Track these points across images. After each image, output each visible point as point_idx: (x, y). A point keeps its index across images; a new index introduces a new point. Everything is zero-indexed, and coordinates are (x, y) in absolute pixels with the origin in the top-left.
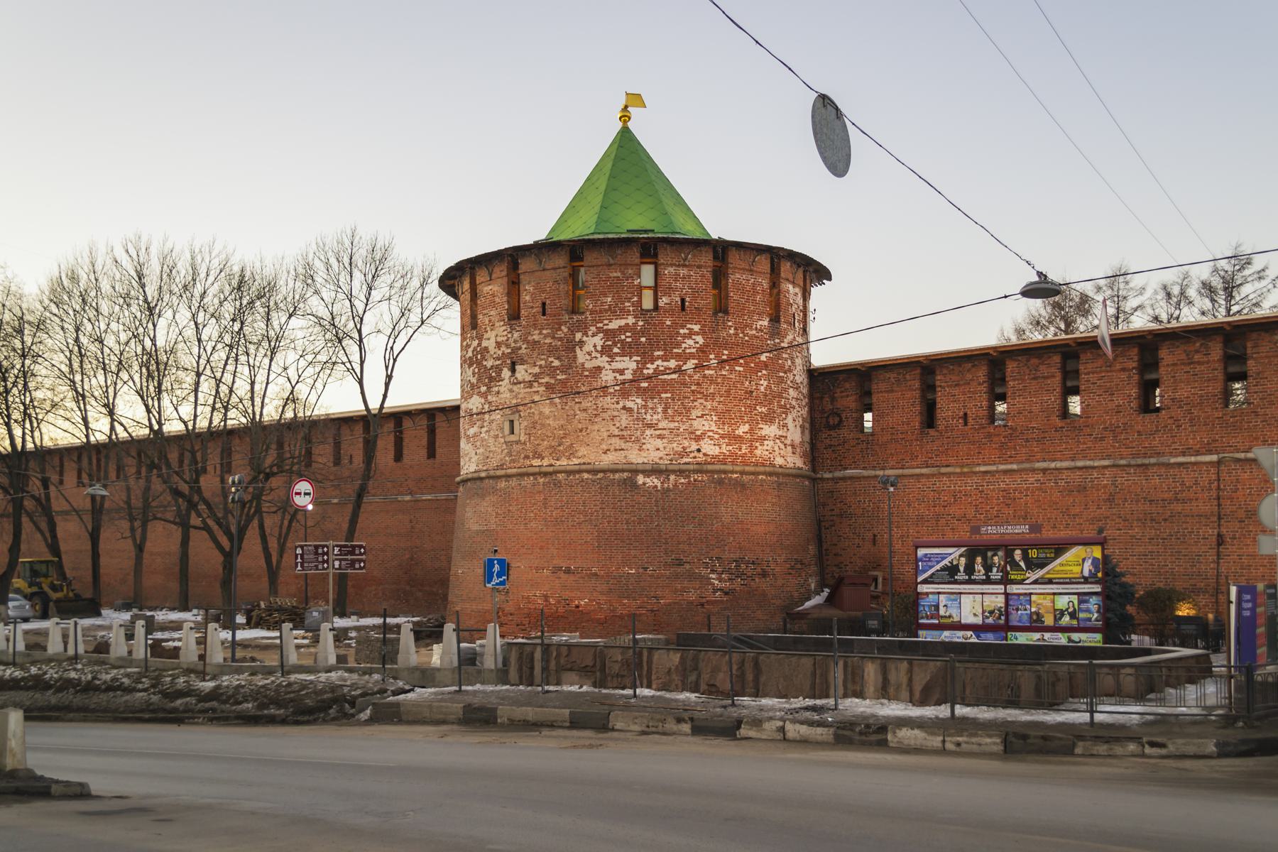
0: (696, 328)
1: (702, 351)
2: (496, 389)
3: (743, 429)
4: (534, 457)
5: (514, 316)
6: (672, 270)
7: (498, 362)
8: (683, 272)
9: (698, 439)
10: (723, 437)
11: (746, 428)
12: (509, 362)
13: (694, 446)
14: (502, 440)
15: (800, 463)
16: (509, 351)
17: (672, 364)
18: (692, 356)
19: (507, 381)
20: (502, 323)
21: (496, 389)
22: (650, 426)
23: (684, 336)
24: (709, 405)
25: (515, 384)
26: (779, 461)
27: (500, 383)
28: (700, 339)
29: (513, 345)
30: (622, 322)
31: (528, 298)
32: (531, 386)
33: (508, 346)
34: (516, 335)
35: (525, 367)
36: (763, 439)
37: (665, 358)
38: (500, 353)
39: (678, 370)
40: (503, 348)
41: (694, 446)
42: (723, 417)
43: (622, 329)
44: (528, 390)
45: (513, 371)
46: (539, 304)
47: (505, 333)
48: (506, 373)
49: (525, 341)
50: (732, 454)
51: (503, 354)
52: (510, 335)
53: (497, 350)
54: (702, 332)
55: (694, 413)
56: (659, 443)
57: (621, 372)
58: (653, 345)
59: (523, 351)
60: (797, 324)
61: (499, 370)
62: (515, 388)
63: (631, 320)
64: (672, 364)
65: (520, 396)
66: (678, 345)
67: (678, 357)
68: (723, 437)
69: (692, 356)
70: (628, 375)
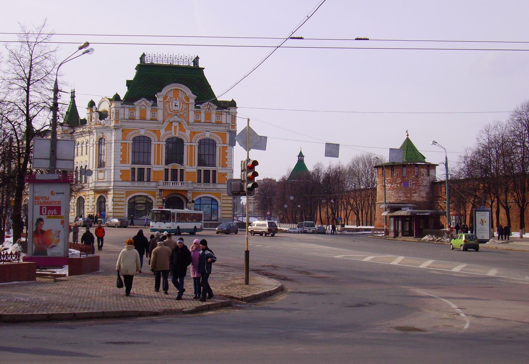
0: (400, 179)
1: (401, 183)
3: (409, 195)
6: (396, 169)
8: (397, 169)
9: (400, 197)
10: (405, 197)
11: (409, 195)
13: (399, 199)
15: (424, 200)
17: (396, 185)
18: (398, 184)
22: (392, 195)
23: (398, 180)
24: (402, 191)
26: (417, 200)
28: (400, 180)
30: (389, 178)
36: (414, 196)
37: (395, 184)
39: (397, 186)
41: (399, 199)
42: (404, 194)
43: (389, 179)
50: (406, 200)
54: (401, 179)
55: (399, 193)
56: (393, 198)
57: (388, 186)
58: (393, 182)
60: (424, 175)
63: (390, 178)
64: (396, 185)
66: (397, 182)
67: (397, 184)
68: (405, 197)
69: (398, 184)
70: (389, 187)
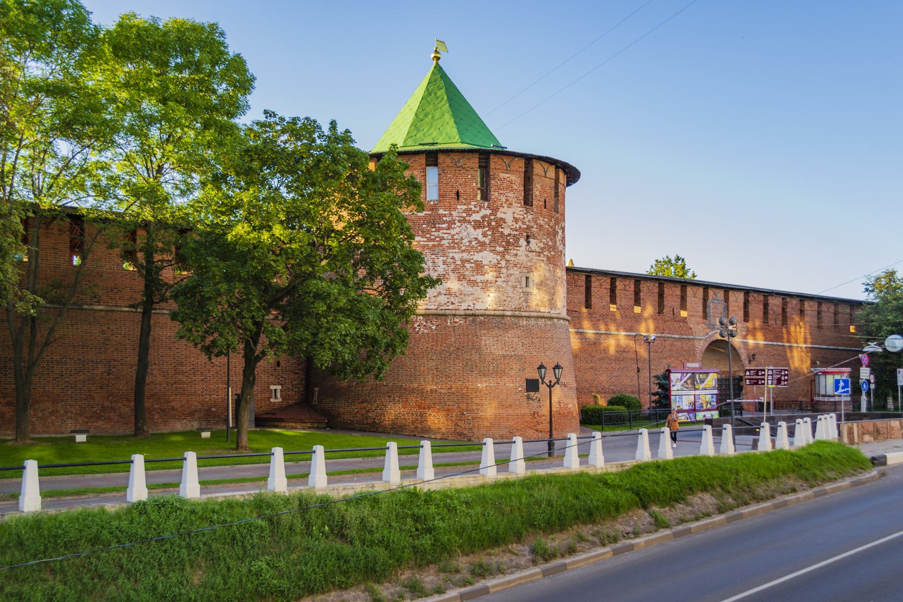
2: (515, 252)
4: (541, 306)
5: (527, 201)
7: (515, 233)
12: (525, 234)
14: (521, 290)
16: (525, 226)
19: (523, 248)
20: (519, 205)
21: (515, 252)
25: (530, 251)
27: (518, 248)
29: (527, 223)
31: (537, 193)
32: (539, 256)
33: (524, 223)
34: (530, 217)
35: (536, 241)
38: (518, 226)
40: (520, 223)
44: (538, 258)
45: (528, 242)
46: (543, 200)
47: (522, 213)
48: (522, 242)
49: (535, 222)
51: (520, 227)
52: (525, 216)
53: (514, 223)
59: (534, 229)
61: (517, 240)
62: (530, 254)
65: (533, 261)
